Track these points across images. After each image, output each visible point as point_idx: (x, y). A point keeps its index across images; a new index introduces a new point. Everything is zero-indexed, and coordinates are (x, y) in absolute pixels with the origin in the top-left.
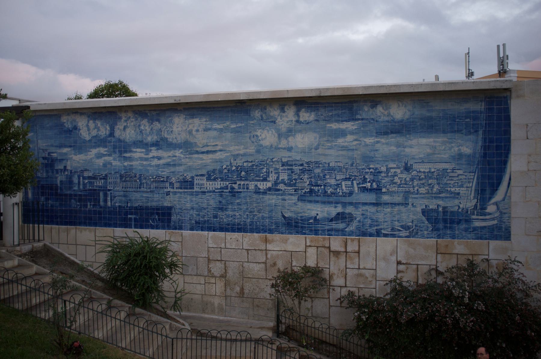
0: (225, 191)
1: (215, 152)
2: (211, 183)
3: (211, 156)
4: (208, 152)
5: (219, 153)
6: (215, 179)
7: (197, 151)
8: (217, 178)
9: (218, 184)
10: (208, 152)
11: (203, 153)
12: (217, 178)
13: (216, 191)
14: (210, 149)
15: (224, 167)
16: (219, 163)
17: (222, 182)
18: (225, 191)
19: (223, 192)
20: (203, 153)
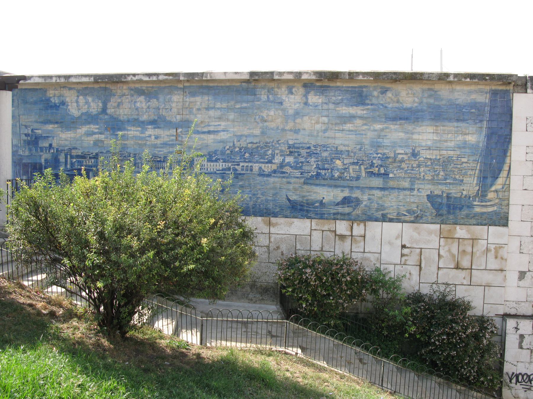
0: (227, 172)
1: (218, 132)
2: (212, 164)
3: (212, 136)
4: (209, 132)
5: (222, 133)
6: (216, 161)
7: (198, 131)
8: (219, 159)
9: (221, 165)
10: (209, 132)
11: (204, 133)
12: (219, 159)
13: (218, 172)
14: (212, 129)
15: (228, 147)
16: (221, 144)
17: (224, 164)
18: (227, 172)
19: (225, 173)
20: (204, 133)
